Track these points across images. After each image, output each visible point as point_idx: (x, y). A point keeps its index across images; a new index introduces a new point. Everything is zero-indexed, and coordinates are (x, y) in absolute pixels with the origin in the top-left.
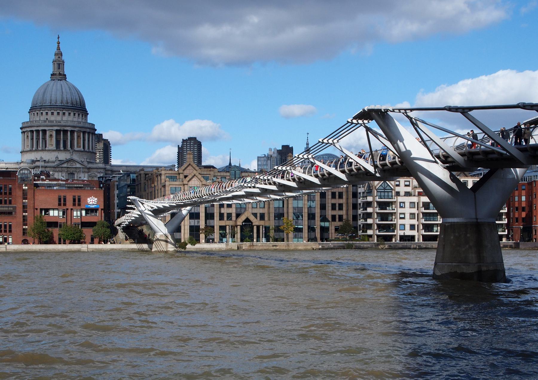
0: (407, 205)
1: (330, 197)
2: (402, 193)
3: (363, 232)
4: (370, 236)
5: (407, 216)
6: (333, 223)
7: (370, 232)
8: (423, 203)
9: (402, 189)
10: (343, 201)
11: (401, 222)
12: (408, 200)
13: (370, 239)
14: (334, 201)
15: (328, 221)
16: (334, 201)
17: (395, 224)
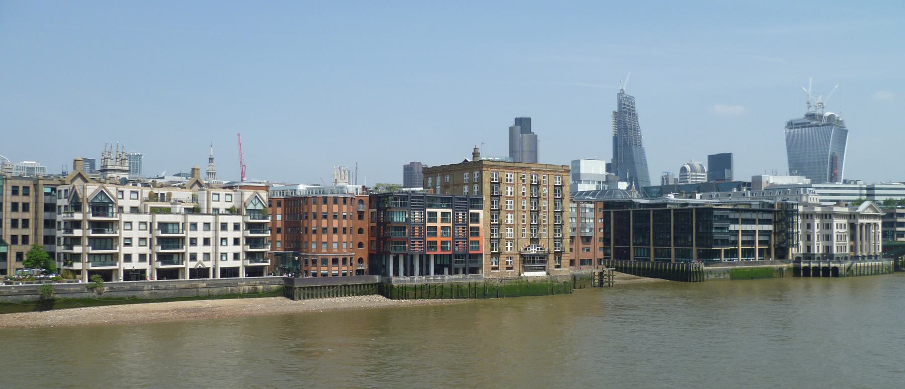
0: (135, 225)
1: (9, 209)
2: (127, 209)
3: (65, 264)
4: (78, 272)
5: (135, 242)
6: (14, 247)
7: (77, 266)
8: (160, 224)
9: (127, 203)
10: (29, 215)
11: (126, 250)
12: (135, 218)
13: (78, 276)
14: (15, 215)
15: (6, 245)
16: (15, 215)
17: (117, 254)
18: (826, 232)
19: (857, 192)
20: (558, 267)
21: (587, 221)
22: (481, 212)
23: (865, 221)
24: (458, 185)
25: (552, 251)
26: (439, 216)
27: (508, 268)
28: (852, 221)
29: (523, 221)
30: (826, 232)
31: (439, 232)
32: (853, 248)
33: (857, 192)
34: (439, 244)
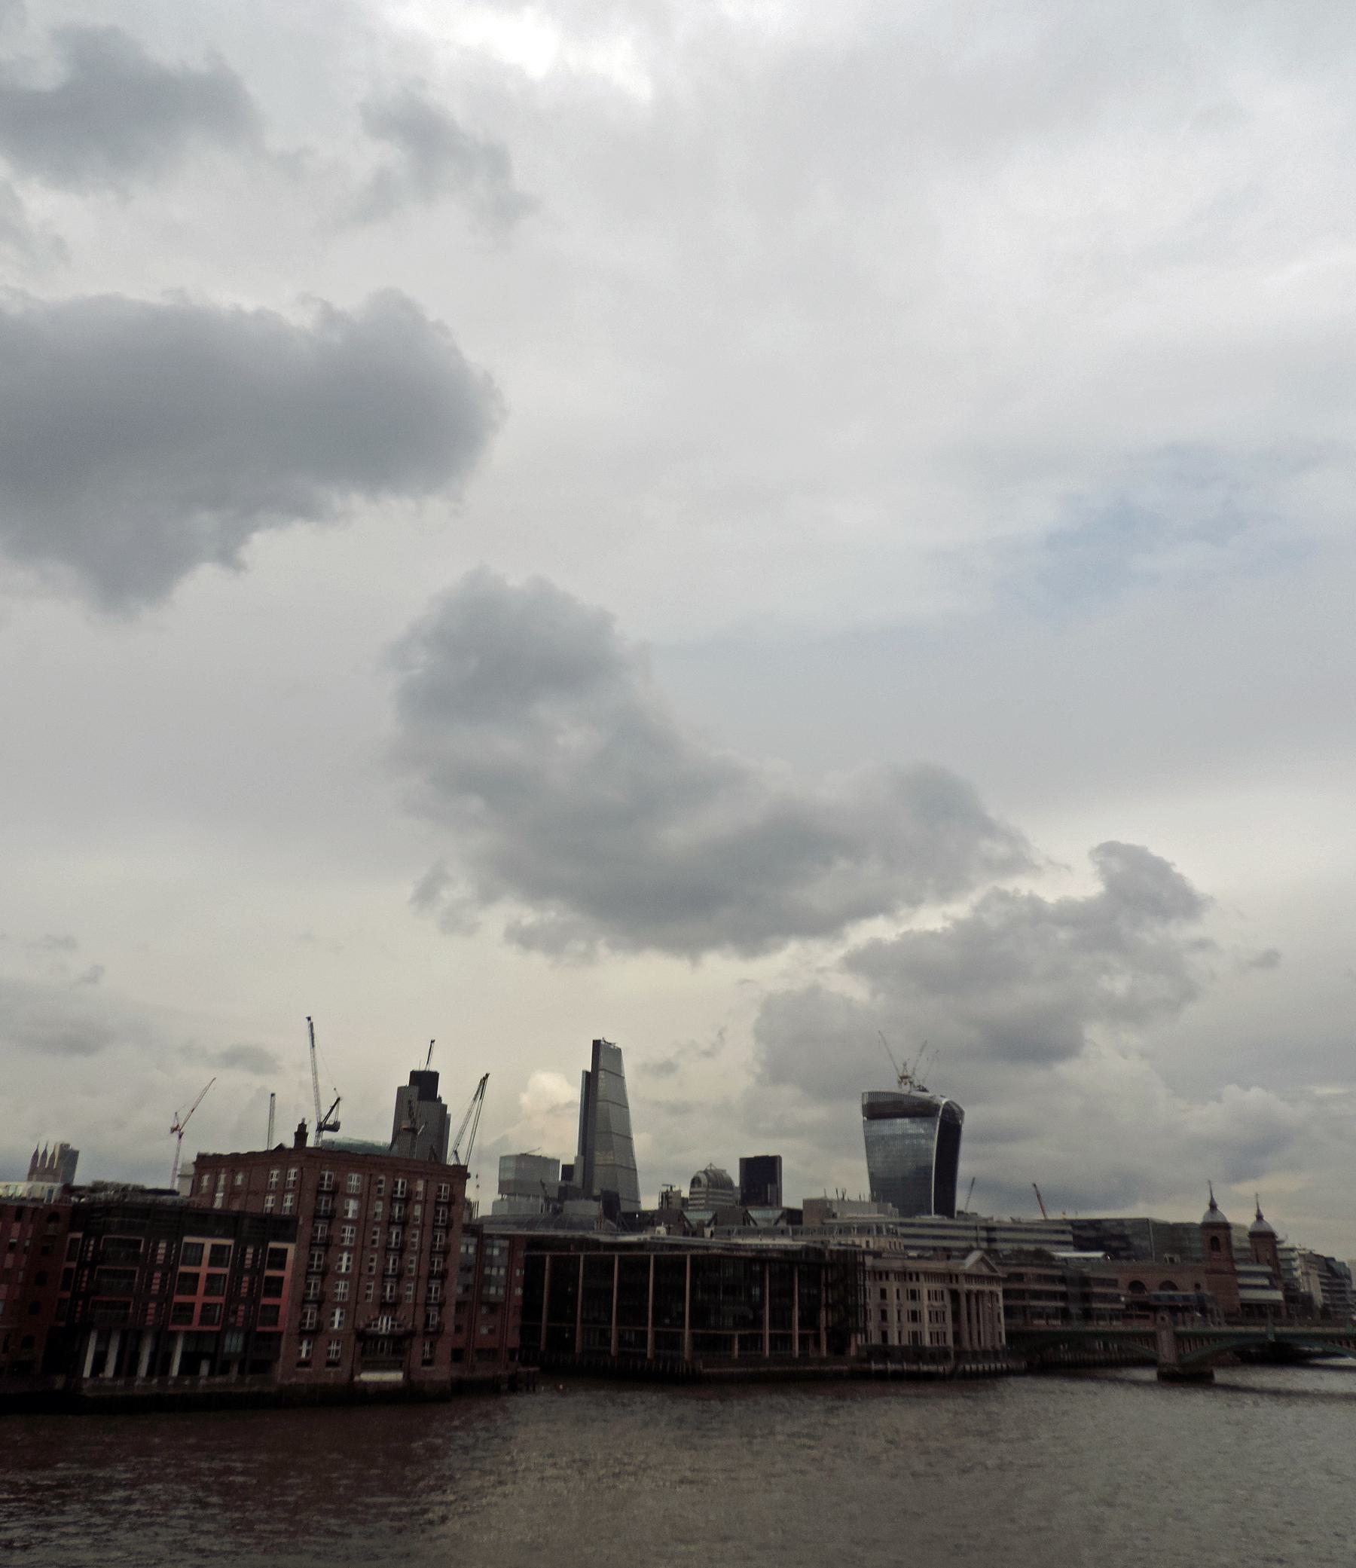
18: (910, 1305)
19: (972, 1234)
20: (427, 1363)
21: (494, 1272)
22: (291, 1248)
23: (975, 1287)
24: (256, 1193)
25: (420, 1326)
26: (207, 1252)
27: (331, 1364)
28: (954, 1286)
29: (371, 1269)
30: (910, 1305)
31: (202, 1285)
32: (957, 1337)
33: (972, 1234)
34: (198, 1309)
